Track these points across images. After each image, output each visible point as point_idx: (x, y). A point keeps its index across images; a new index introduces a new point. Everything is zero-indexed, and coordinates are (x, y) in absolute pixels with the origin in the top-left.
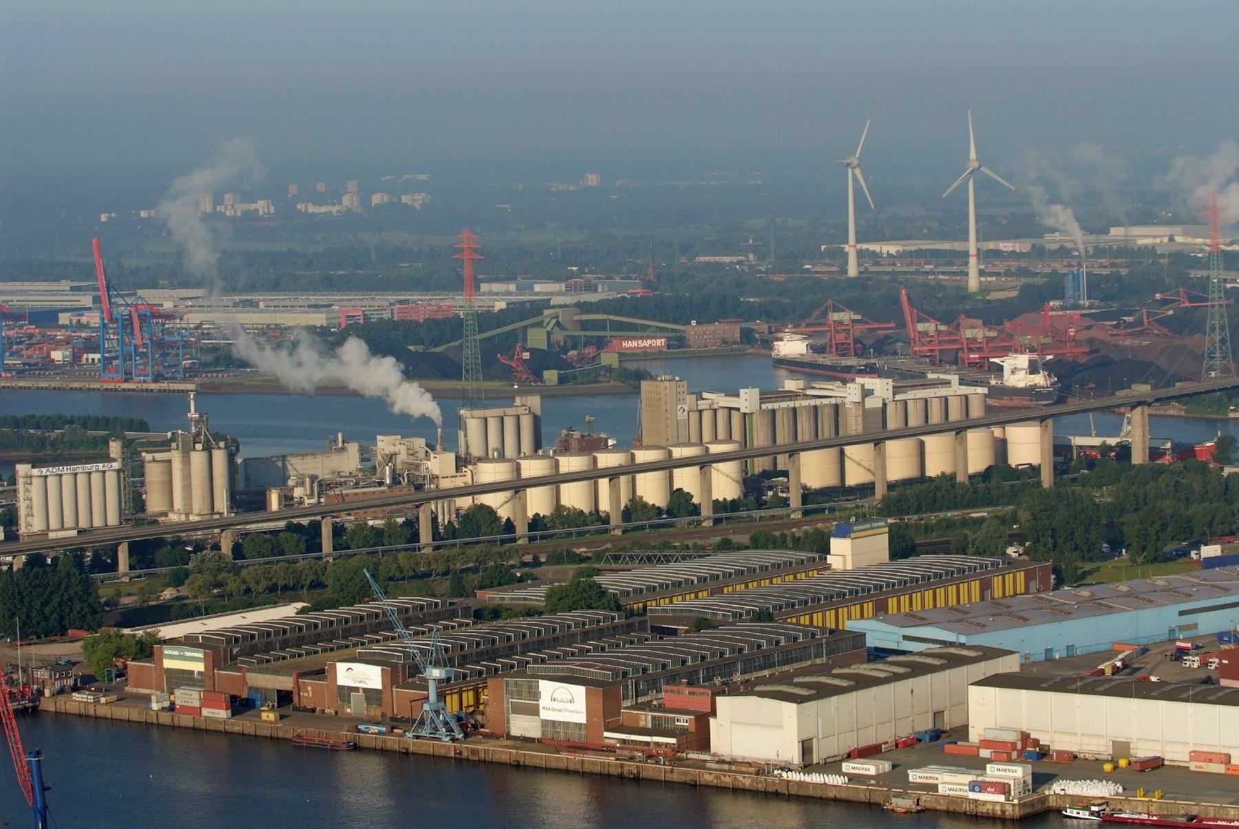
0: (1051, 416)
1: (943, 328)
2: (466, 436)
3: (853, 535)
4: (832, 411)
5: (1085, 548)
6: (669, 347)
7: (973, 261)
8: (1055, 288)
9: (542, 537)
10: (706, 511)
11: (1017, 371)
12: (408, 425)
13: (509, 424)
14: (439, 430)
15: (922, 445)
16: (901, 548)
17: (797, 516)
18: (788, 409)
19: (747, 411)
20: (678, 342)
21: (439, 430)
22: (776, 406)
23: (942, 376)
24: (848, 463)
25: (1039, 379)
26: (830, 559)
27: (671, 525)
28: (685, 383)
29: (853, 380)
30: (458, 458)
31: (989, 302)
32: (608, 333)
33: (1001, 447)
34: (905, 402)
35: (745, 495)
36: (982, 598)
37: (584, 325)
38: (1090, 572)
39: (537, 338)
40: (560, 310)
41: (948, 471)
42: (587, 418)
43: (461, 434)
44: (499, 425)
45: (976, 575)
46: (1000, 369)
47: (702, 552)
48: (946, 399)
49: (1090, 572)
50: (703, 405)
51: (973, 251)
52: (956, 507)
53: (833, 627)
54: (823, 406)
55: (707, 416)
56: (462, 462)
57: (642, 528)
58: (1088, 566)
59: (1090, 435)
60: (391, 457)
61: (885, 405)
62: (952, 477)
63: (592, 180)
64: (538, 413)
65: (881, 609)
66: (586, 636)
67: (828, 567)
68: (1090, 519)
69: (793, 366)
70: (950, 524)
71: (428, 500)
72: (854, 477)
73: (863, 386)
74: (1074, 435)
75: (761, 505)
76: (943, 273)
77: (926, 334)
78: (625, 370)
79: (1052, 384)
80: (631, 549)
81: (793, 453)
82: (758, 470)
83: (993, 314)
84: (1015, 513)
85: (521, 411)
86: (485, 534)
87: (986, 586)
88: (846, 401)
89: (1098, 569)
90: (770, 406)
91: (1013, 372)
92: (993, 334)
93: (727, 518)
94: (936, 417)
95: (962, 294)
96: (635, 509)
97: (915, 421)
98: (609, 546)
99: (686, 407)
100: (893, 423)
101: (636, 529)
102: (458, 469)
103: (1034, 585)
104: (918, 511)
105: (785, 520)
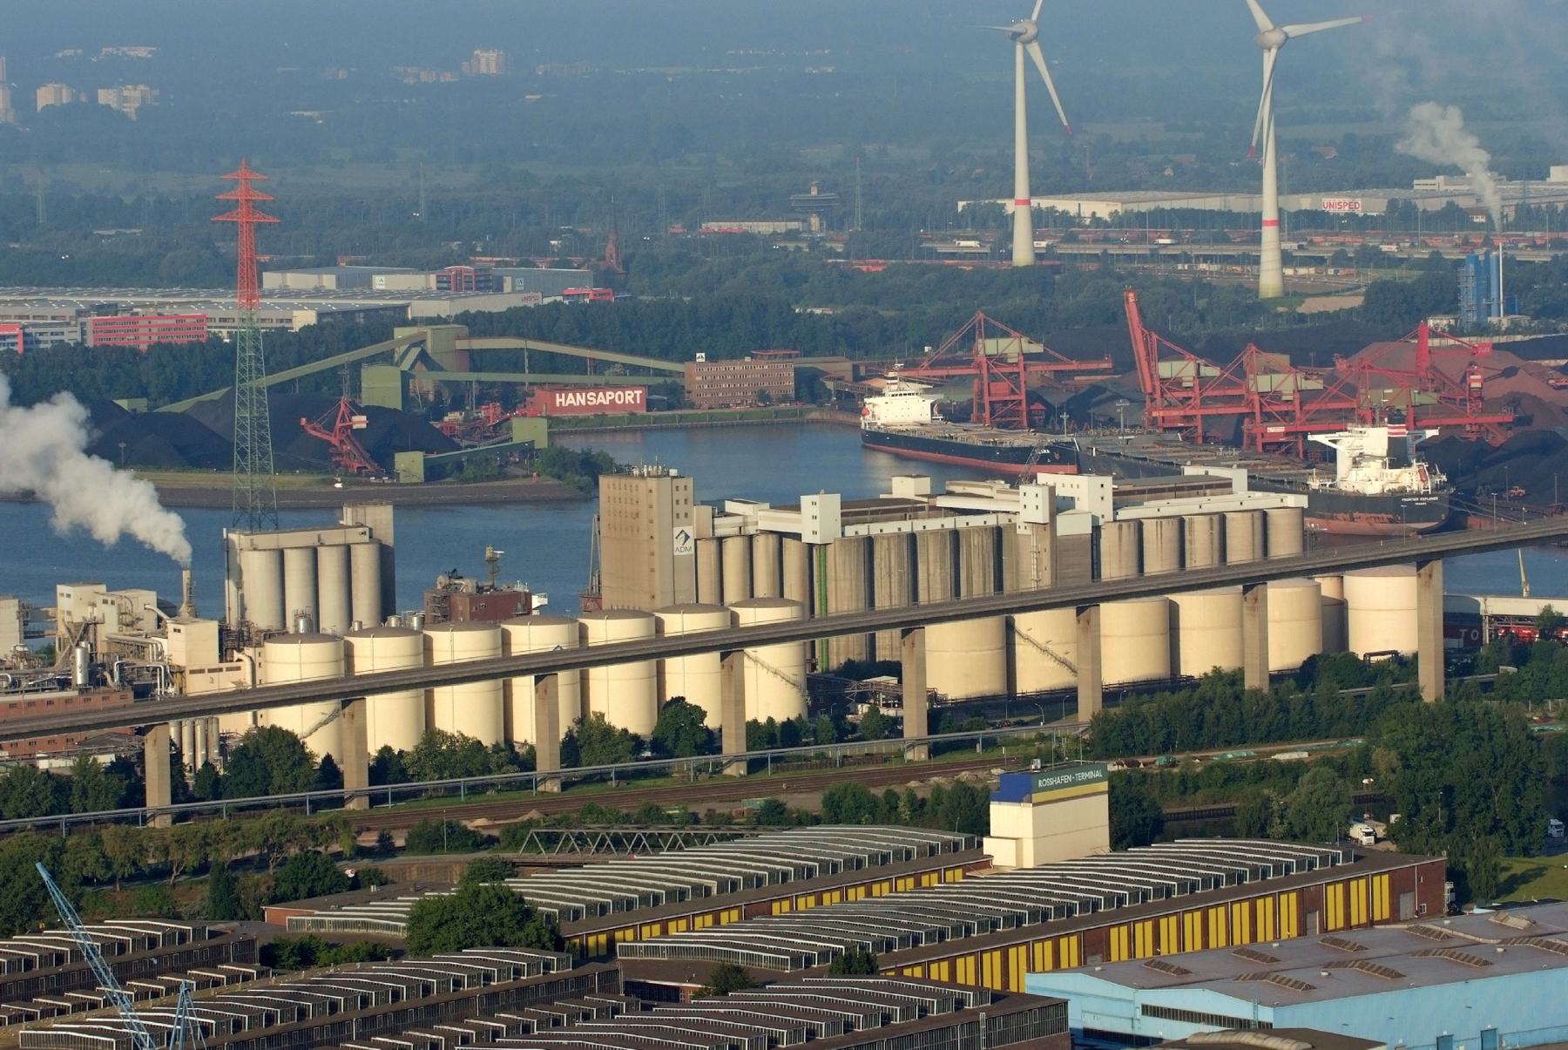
0: (1439, 555)
1: (1211, 371)
2: (239, 586)
3: (1036, 797)
4: (988, 542)
5: (1512, 826)
6: (650, 405)
7: (1269, 235)
8: (1439, 289)
9: (398, 797)
10: (733, 745)
11: (1365, 461)
12: (126, 562)
13: (330, 563)
14: (186, 575)
15: (1173, 612)
16: (1134, 824)
17: (919, 755)
18: (899, 536)
19: (816, 540)
20: (668, 395)
21: (186, 575)
22: (874, 529)
23: (1214, 472)
24: (1021, 649)
25: (1410, 478)
26: (989, 846)
27: (662, 773)
28: (689, 482)
29: (1032, 479)
30: (223, 632)
31: (1302, 318)
32: (526, 377)
33: (1335, 618)
34: (1139, 525)
35: (812, 710)
36: (1303, 930)
37: (476, 361)
38: (1525, 878)
39: (380, 387)
40: (428, 330)
41: (1227, 664)
42: (488, 554)
43: (230, 587)
44: (309, 565)
45: (1290, 881)
46: (1328, 457)
47: (725, 829)
48: (1222, 517)
49: (1525, 878)
50: (725, 526)
51: (1269, 214)
52: (1243, 741)
53: (998, 986)
54: (971, 531)
55: (733, 550)
56: (232, 641)
57: (603, 778)
58: (1520, 866)
59: (1518, 594)
60: (86, 629)
61: (1097, 529)
62: (1236, 678)
63: (488, 61)
64: (389, 540)
65: (1094, 949)
66: (492, 1003)
67: (986, 863)
68: (1525, 768)
69: (904, 447)
70: (1232, 775)
71: (165, 718)
72: (1034, 676)
73: (1052, 489)
74: (1486, 593)
75: (843, 732)
76: (1207, 259)
77: (1176, 383)
78: (563, 452)
79: (1437, 488)
80: (581, 823)
81: (910, 627)
82: (836, 661)
83: (1314, 343)
84: (1365, 754)
85: (354, 536)
86: (280, 790)
87: (1310, 904)
88: (1018, 521)
89: (1539, 872)
90: (863, 530)
91: (1355, 464)
92: (1315, 384)
93: (775, 760)
94: (1200, 556)
95: (1249, 304)
96: (587, 741)
97: (1158, 562)
98: (534, 814)
99: (690, 530)
100: (1113, 567)
101: (587, 780)
102: (223, 655)
103: (1408, 904)
104: (1165, 748)
105: (893, 765)
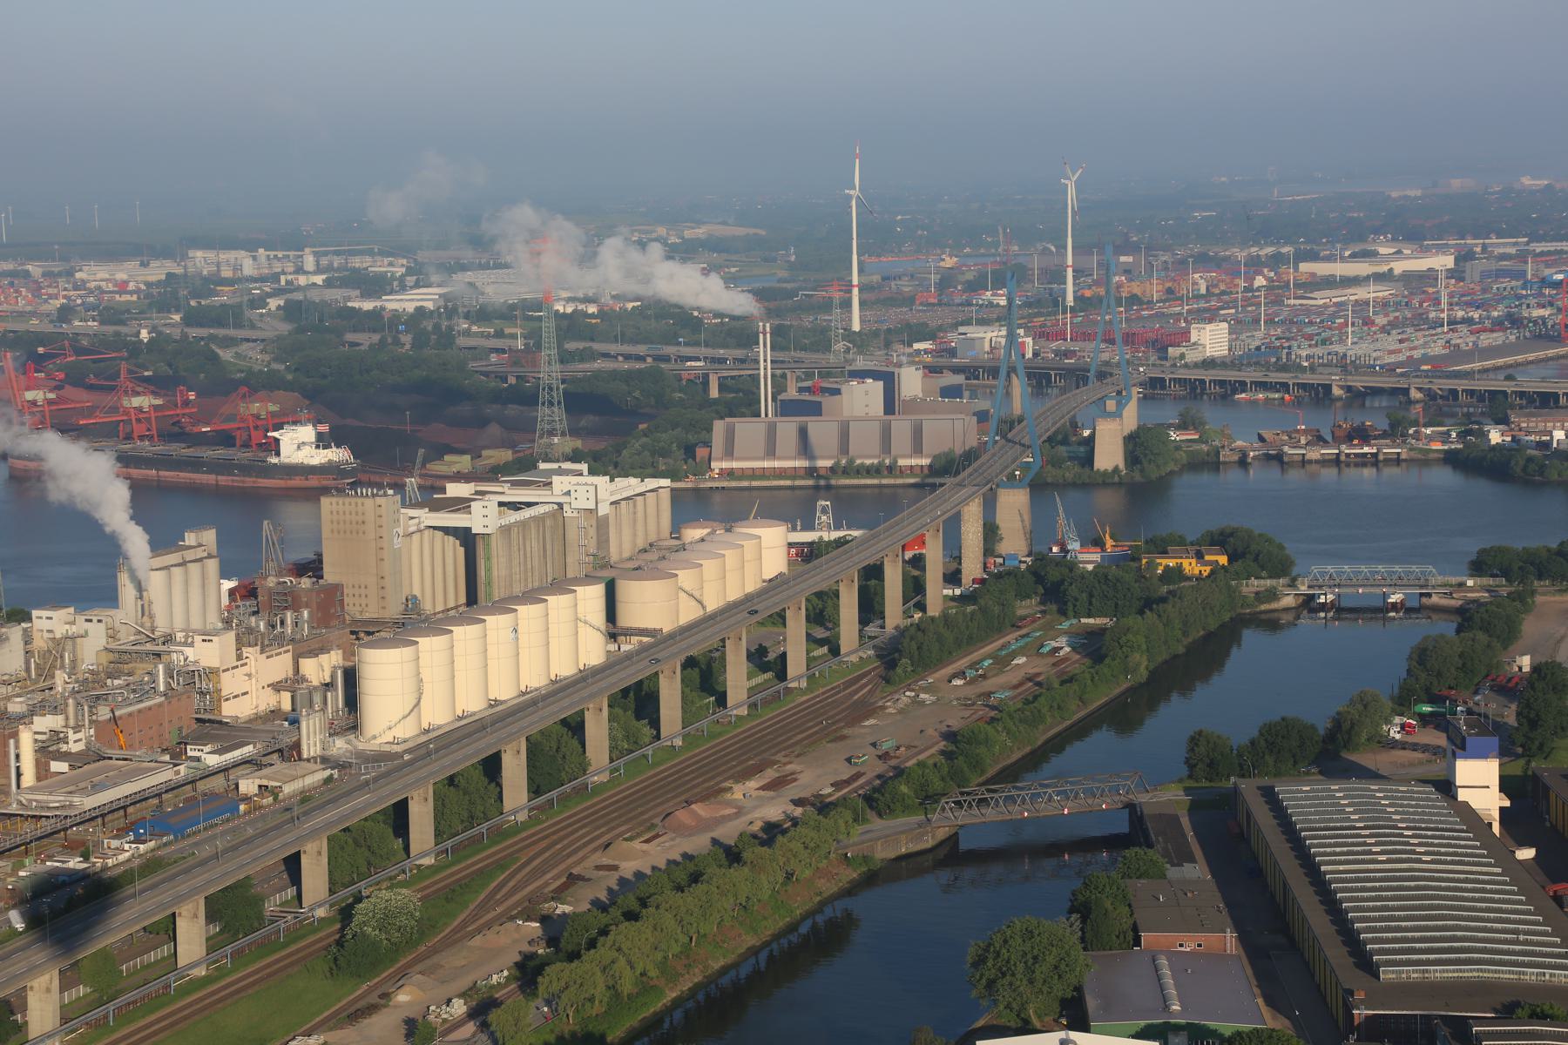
1: (52, 396)
46: (275, 446)
85: (200, 553)
92: (159, 402)
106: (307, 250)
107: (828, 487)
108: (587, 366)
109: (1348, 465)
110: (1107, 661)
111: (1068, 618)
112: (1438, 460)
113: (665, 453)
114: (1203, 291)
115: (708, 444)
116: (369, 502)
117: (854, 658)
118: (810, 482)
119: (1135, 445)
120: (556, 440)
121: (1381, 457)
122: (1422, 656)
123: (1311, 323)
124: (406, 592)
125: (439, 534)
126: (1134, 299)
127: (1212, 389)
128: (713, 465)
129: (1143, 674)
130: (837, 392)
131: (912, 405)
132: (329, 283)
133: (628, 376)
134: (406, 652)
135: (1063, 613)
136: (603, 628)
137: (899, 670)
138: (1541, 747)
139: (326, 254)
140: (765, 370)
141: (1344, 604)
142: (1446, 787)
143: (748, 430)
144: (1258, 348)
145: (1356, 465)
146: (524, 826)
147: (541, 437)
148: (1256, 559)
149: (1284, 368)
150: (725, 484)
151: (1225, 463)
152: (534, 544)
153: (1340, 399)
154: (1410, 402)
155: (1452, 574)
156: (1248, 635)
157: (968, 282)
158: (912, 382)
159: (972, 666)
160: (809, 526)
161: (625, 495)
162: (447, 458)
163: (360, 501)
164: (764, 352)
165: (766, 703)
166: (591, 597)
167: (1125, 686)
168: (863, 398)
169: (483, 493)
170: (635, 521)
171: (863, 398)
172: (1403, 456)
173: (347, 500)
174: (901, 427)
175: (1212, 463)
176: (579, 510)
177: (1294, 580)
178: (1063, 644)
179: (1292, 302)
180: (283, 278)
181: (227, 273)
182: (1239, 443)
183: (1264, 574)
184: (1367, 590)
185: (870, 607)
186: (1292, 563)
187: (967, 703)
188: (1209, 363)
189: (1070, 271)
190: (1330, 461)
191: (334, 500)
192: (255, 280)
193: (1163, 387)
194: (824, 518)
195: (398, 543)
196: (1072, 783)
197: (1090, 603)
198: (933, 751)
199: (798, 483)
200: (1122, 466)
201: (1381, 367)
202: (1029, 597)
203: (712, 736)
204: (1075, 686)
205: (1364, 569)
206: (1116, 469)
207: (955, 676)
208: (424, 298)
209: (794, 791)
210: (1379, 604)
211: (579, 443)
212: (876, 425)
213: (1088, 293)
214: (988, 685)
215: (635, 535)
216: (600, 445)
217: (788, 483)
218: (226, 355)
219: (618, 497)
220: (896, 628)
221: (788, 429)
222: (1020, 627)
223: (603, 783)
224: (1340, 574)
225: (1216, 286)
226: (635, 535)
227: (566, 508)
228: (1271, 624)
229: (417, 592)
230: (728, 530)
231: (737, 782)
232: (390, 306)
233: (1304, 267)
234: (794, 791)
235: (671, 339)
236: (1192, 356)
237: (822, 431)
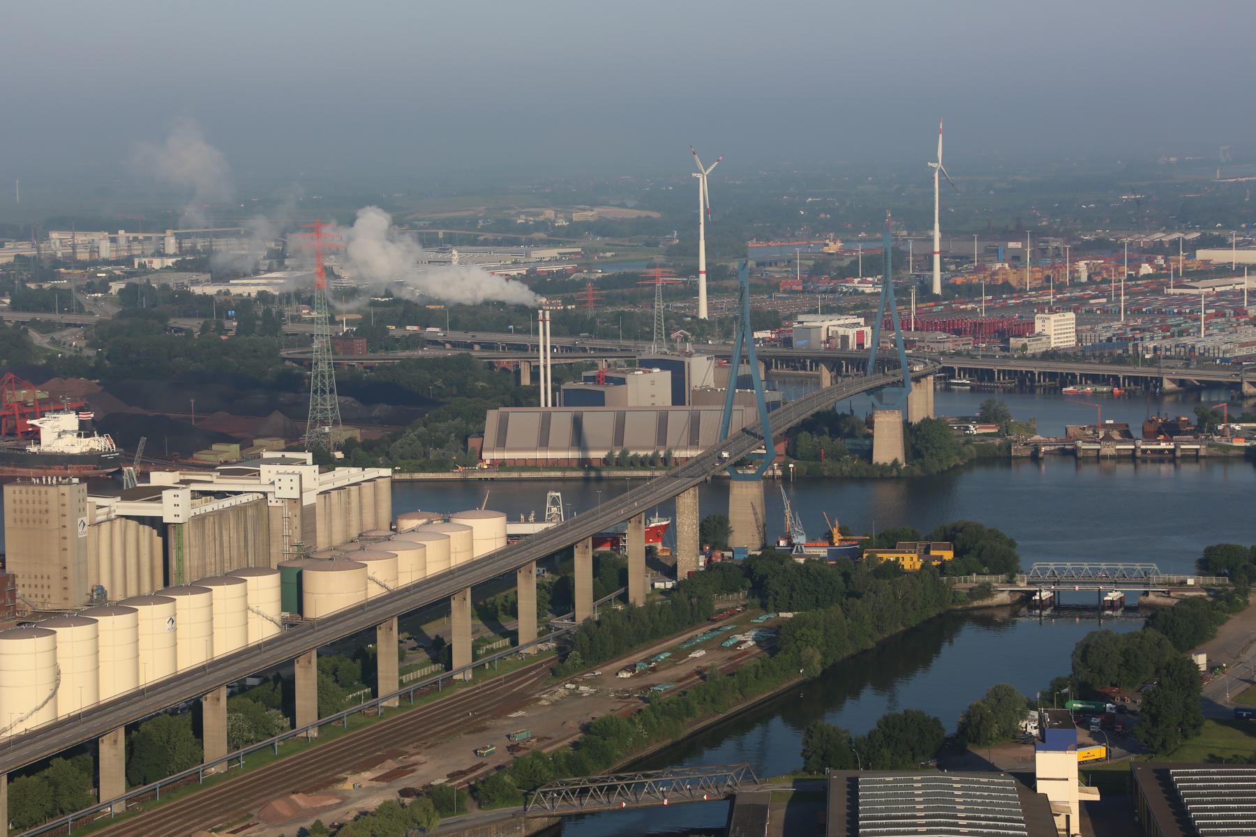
25: (99, 443)
46: (35, 435)
50: (101, 515)
106: (169, 232)
107: (599, 479)
108: (407, 354)
109: (1144, 461)
110: (780, 655)
111: (767, 612)
112: (1239, 457)
113: (439, 444)
114: (1084, 278)
115: (481, 434)
116: (52, 491)
117: (531, 650)
118: (580, 474)
119: (917, 437)
120: (327, 429)
121: (1178, 453)
122: (1084, 652)
123: (1180, 313)
124: (92, 582)
125: (132, 524)
126: (1007, 288)
127: (1048, 381)
128: (485, 455)
129: (818, 669)
130: (622, 381)
131: (704, 396)
132: (180, 267)
133: (444, 363)
134: (41, 643)
135: (764, 607)
136: (277, 619)
137: (568, 663)
138: (1163, 745)
139: (188, 236)
140: (545, 360)
141: (1064, 601)
142: (1028, 779)
143: (522, 420)
144: (1109, 340)
145: (1153, 461)
146: (119, 817)
147: (313, 427)
148: (979, 555)
149: (1120, 361)
150: (494, 475)
151: (1016, 458)
152: (231, 534)
153: (1171, 393)
154: (1243, 397)
155: (1177, 573)
156: (969, 634)
157: (840, 268)
158: (702, 371)
159: (647, 661)
160: (540, 519)
161: (338, 485)
162: (215, 447)
163: (43, 489)
164: (545, 339)
165: (420, 693)
166: (264, 591)
167: (796, 681)
168: (648, 388)
169: (187, 482)
170: (347, 511)
171: (648, 388)
172: (1202, 453)
173: (31, 489)
174: (679, 419)
175: (1000, 458)
176: (283, 499)
177: (1012, 576)
178: (748, 640)
179: (1172, 291)
180: (136, 261)
181: (83, 255)
182: (1037, 437)
183: (985, 570)
184: (1084, 588)
185: (558, 597)
186: (1016, 559)
187: (624, 696)
188: (1052, 355)
189: (937, 258)
190: (1189, 456)
191: (17, 488)
192: (117, 262)
193: (991, 379)
194: (554, 509)
195: (82, 532)
196: (675, 774)
197: (791, 597)
198: (566, 742)
199: (568, 474)
200: (901, 459)
201: (1223, 360)
202: (736, 590)
203: (352, 727)
204: (735, 680)
205: (1086, 566)
206: (896, 461)
207: (625, 669)
208: (273, 282)
209: (407, 782)
210: (1093, 601)
211: (356, 433)
212: (653, 418)
213: (959, 280)
214: (652, 678)
215: (347, 525)
216: (376, 434)
217: (559, 474)
218: (37, 338)
219: (330, 486)
220: (588, 620)
221: (562, 419)
222: (715, 621)
223: (218, 775)
224: (1061, 571)
225: (1099, 274)
226: (347, 525)
227: (270, 497)
228: (986, 620)
229: (105, 583)
230: (447, 521)
231: (354, 773)
232: (235, 291)
233: (1201, 254)
234: (407, 782)
235: (500, 327)
236: (1035, 347)
237: (597, 421)
